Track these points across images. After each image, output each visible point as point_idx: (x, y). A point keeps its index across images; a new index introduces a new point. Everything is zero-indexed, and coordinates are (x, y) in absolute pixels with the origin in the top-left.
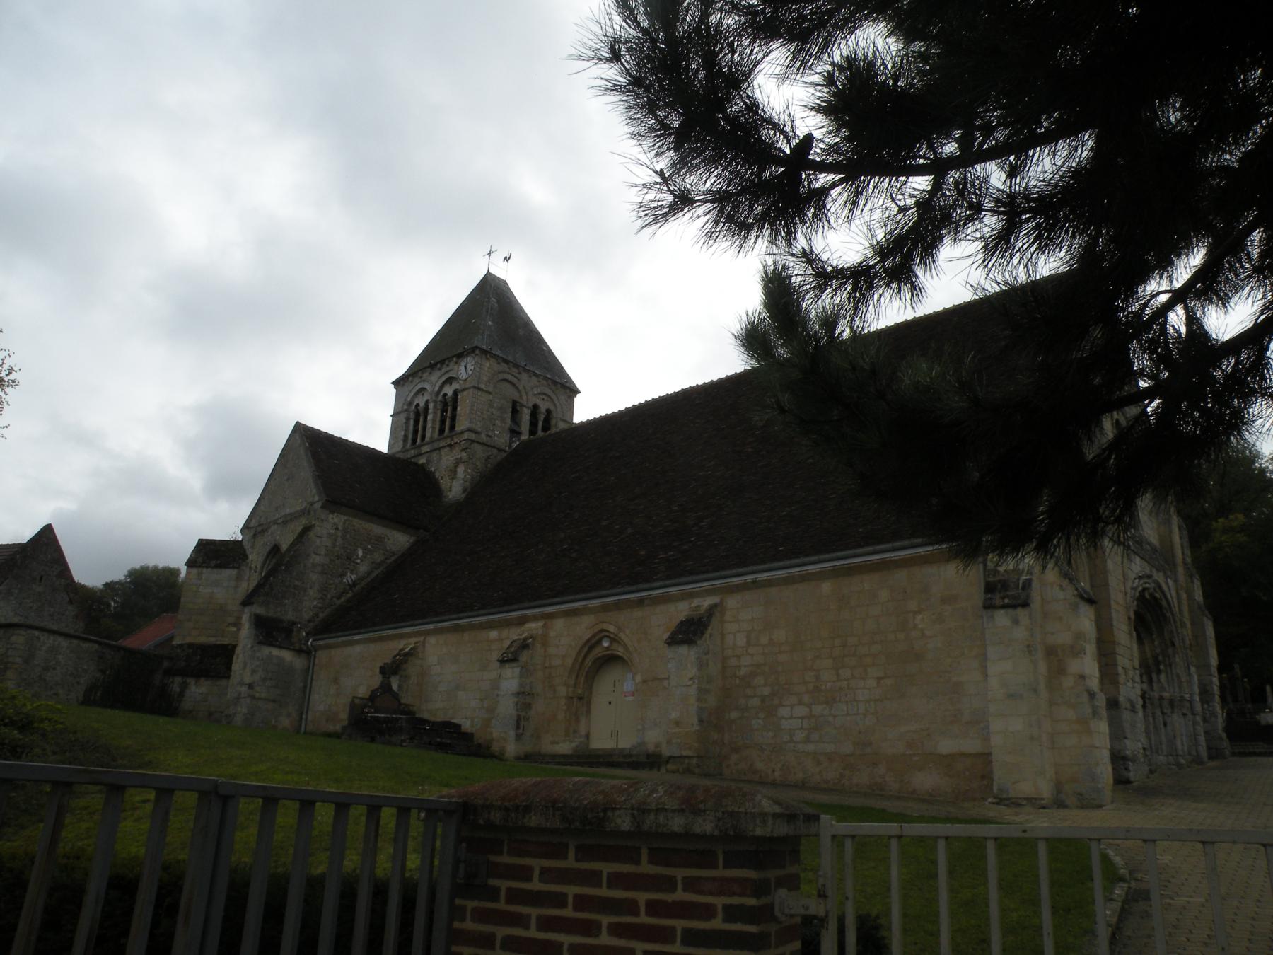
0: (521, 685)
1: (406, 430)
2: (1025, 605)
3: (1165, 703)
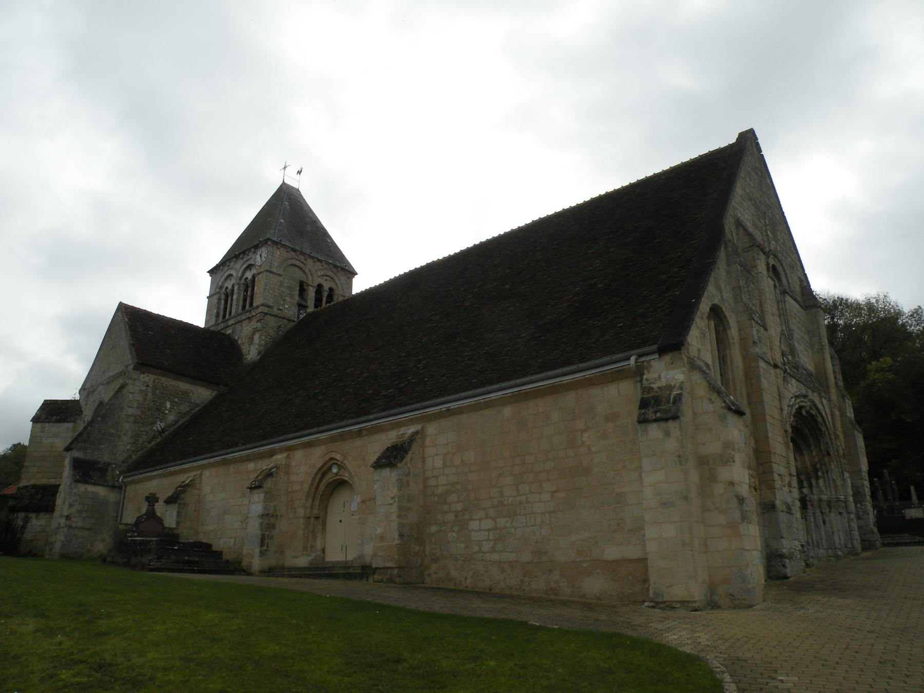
0: (265, 508)
1: (218, 308)
2: (675, 418)
3: (824, 504)
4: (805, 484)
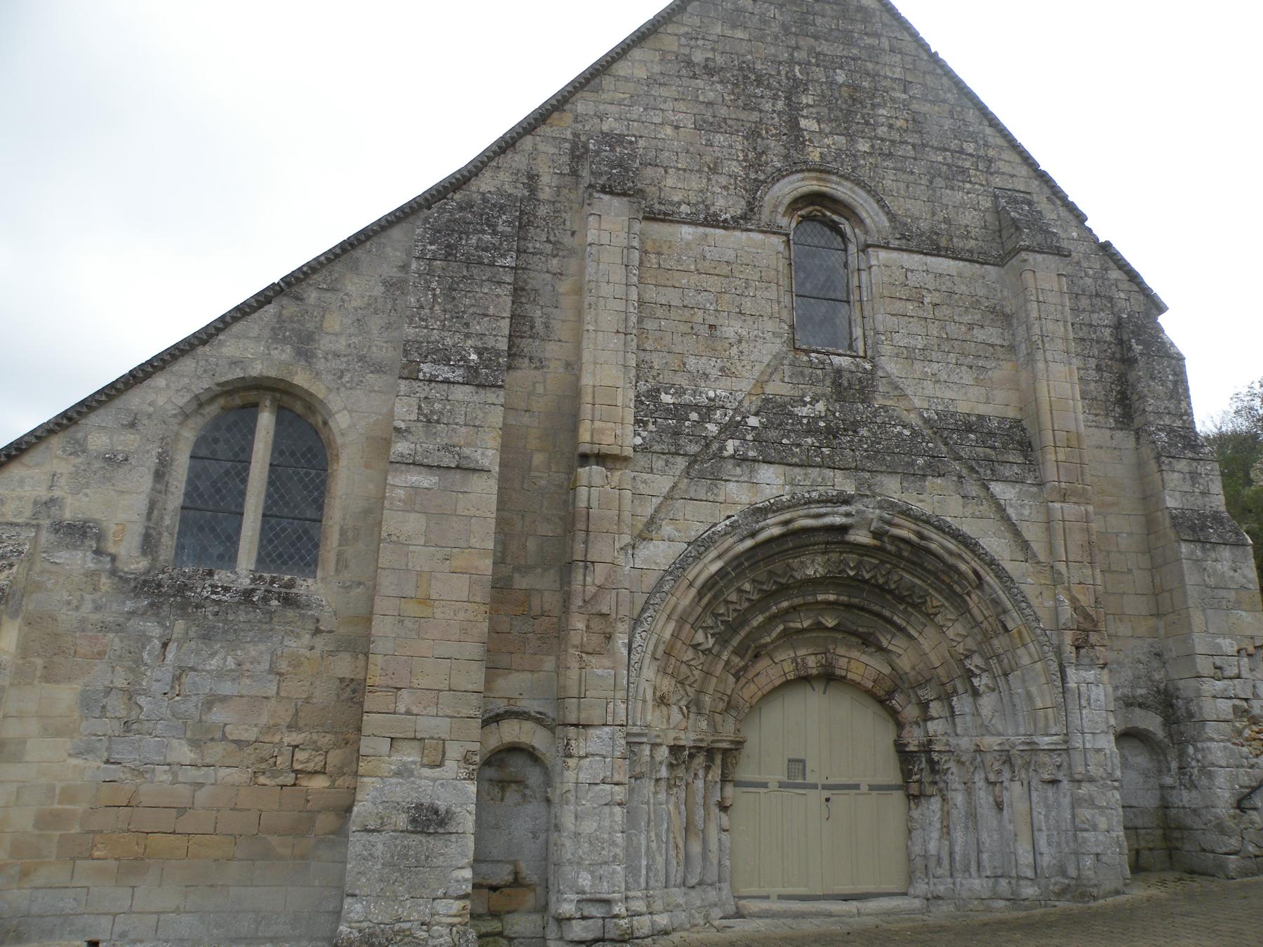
4: (935, 709)
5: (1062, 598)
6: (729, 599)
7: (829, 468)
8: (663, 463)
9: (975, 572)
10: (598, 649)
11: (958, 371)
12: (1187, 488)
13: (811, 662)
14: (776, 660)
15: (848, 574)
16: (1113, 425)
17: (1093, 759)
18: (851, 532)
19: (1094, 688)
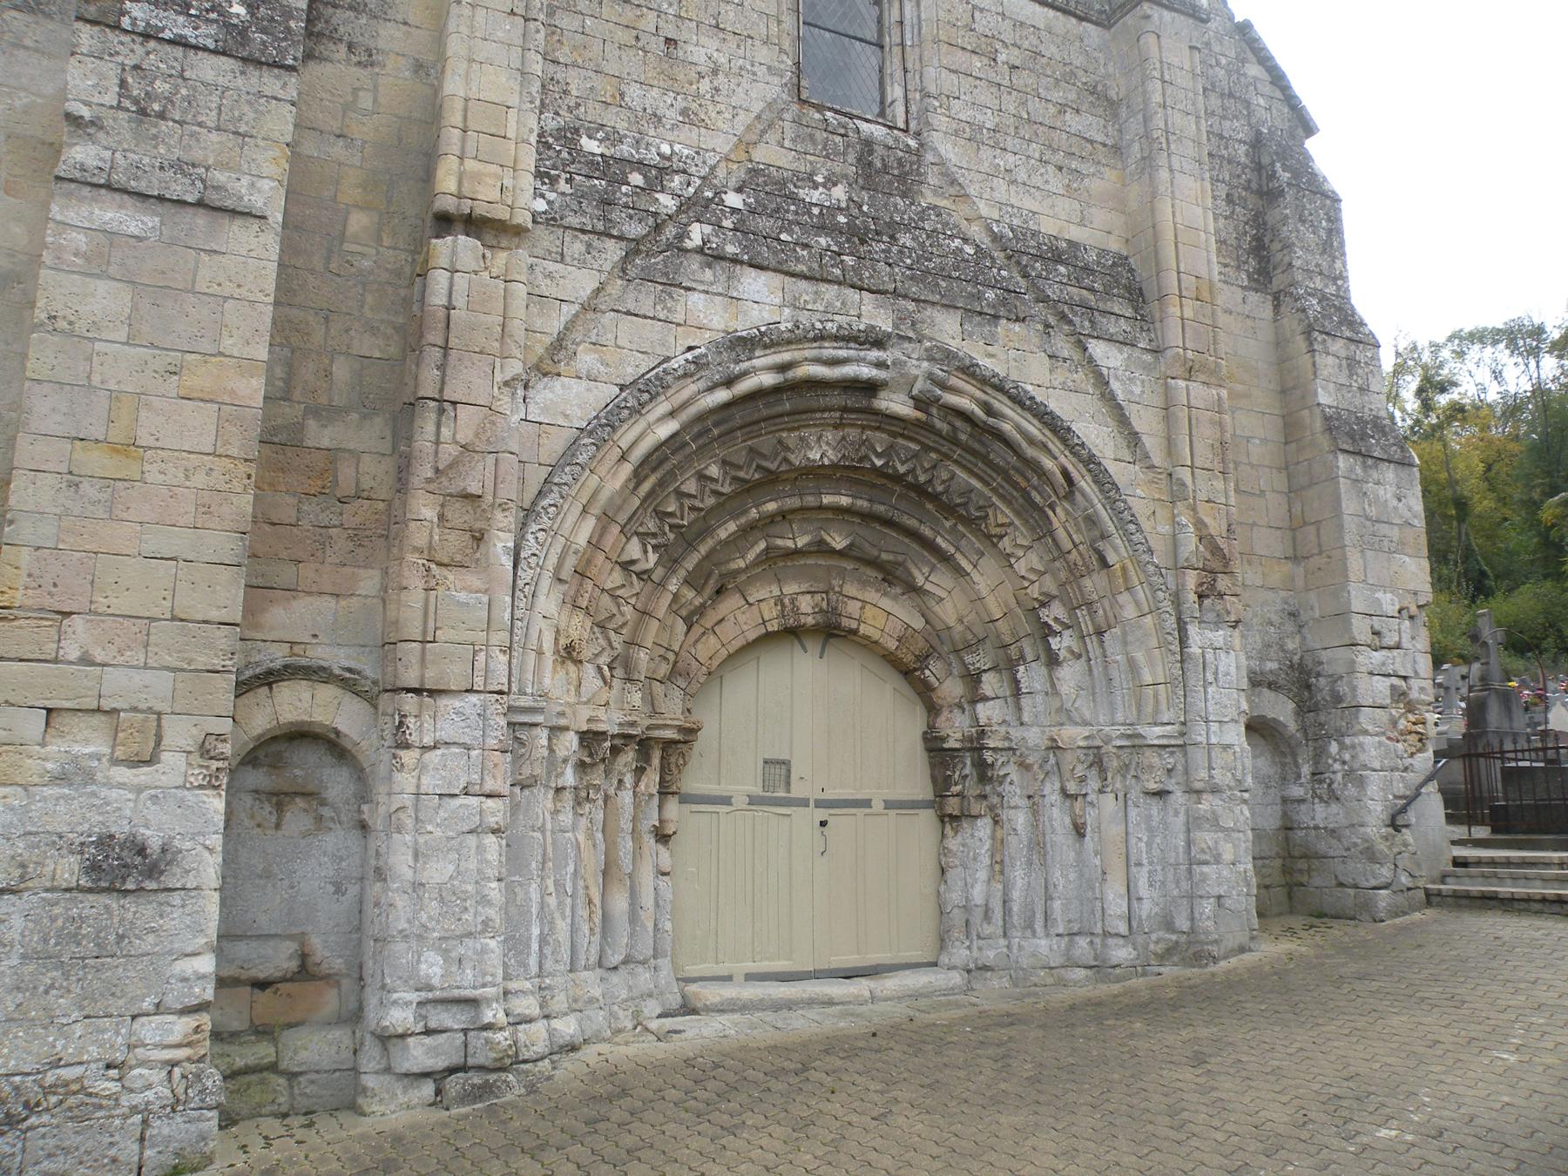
4: (990, 684)
5: (1184, 520)
6: (684, 489)
7: (853, 287)
8: (583, 249)
9: (1066, 473)
10: (458, 558)
11: (1043, 170)
12: (1343, 380)
13: (806, 604)
14: (751, 600)
15: (873, 463)
16: (1246, 283)
17: (1219, 759)
18: (882, 394)
19: (1223, 655)
